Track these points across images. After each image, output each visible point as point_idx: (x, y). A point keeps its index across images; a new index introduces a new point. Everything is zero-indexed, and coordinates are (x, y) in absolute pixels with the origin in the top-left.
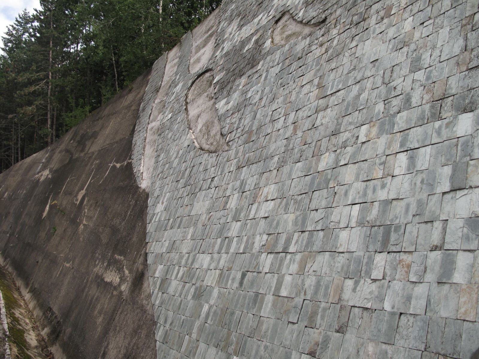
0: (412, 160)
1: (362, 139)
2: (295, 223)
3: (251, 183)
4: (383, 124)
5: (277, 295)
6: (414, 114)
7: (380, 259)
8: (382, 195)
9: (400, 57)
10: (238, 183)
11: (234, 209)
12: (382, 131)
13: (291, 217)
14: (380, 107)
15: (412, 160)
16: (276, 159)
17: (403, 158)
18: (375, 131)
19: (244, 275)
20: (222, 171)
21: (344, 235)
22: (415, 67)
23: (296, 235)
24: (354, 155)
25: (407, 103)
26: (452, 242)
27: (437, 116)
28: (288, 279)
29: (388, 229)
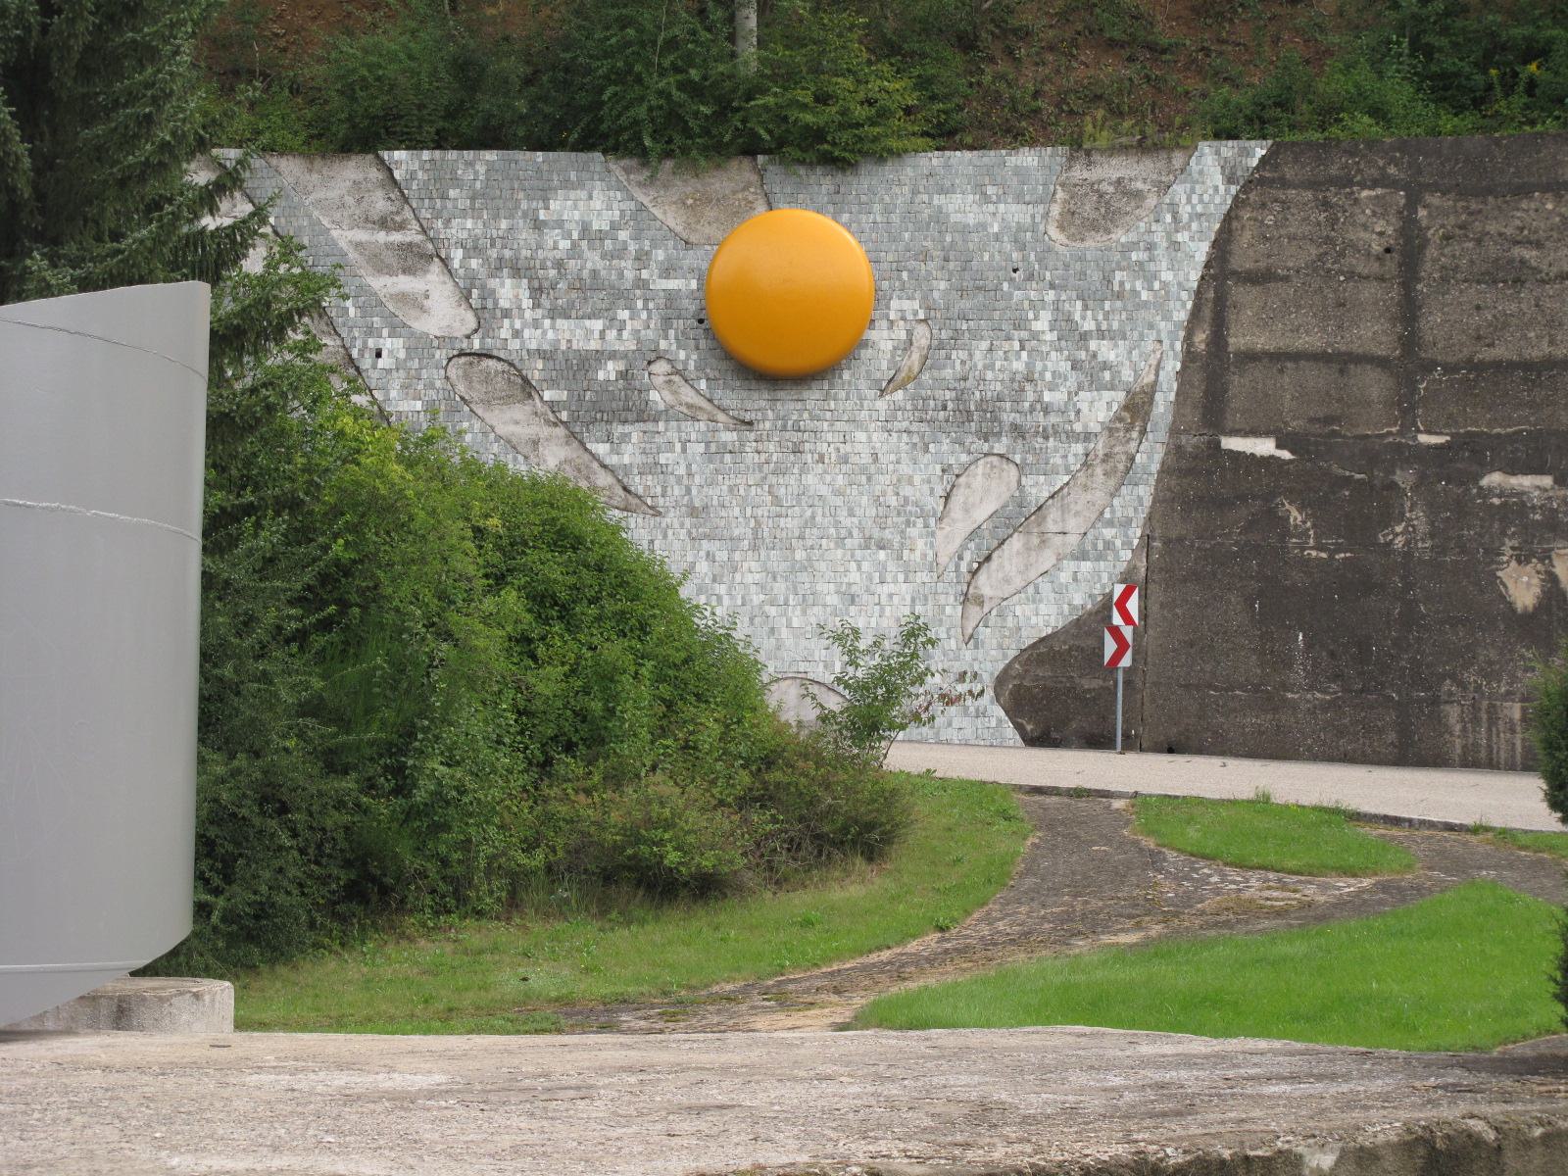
0: (859, 568)
1: (824, 547)
2: (787, 588)
3: (722, 556)
4: (836, 543)
5: (789, 626)
6: (856, 542)
7: (852, 608)
8: (846, 580)
9: (839, 501)
10: (702, 553)
11: (710, 574)
12: (837, 546)
13: (783, 586)
14: (832, 531)
15: (859, 568)
16: (746, 542)
17: (853, 566)
18: (832, 545)
19: (751, 620)
20: (665, 536)
21: (828, 598)
22: (851, 514)
23: (791, 597)
24: (822, 555)
25: (851, 535)
26: (883, 602)
27: (867, 547)
28: (795, 620)
29: (853, 596)
